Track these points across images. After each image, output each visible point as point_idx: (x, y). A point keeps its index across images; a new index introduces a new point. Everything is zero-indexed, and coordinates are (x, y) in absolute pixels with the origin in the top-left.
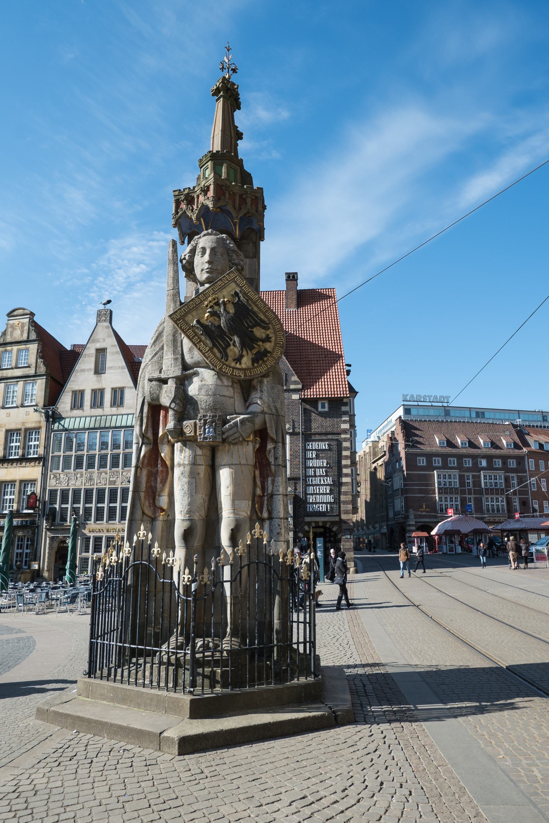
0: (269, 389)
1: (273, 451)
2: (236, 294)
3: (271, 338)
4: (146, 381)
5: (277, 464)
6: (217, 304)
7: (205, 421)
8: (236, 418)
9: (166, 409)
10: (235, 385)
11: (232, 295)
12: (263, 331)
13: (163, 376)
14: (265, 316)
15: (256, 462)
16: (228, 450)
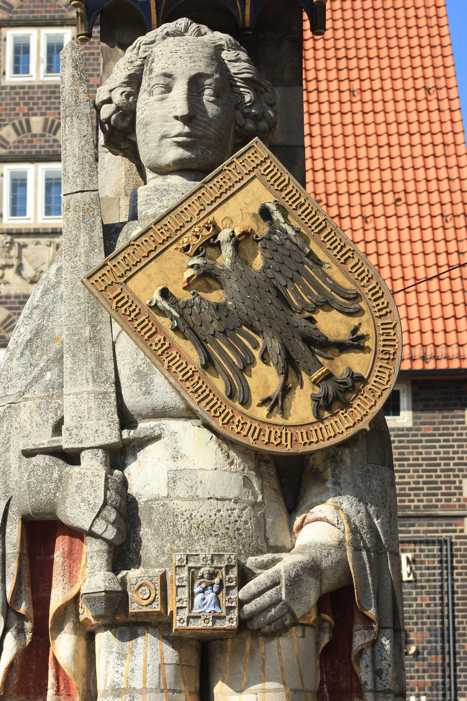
0: (359, 479)
1: (369, 652)
2: (265, 213)
3: (363, 337)
4: (14, 456)
5: (380, 687)
6: (212, 244)
7: (193, 572)
8: (274, 562)
9: (77, 534)
10: (263, 469)
11: (254, 215)
12: (341, 316)
13: (66, 442)
14: (347, 274)
15: (321, 683)
16: (252, 651)
